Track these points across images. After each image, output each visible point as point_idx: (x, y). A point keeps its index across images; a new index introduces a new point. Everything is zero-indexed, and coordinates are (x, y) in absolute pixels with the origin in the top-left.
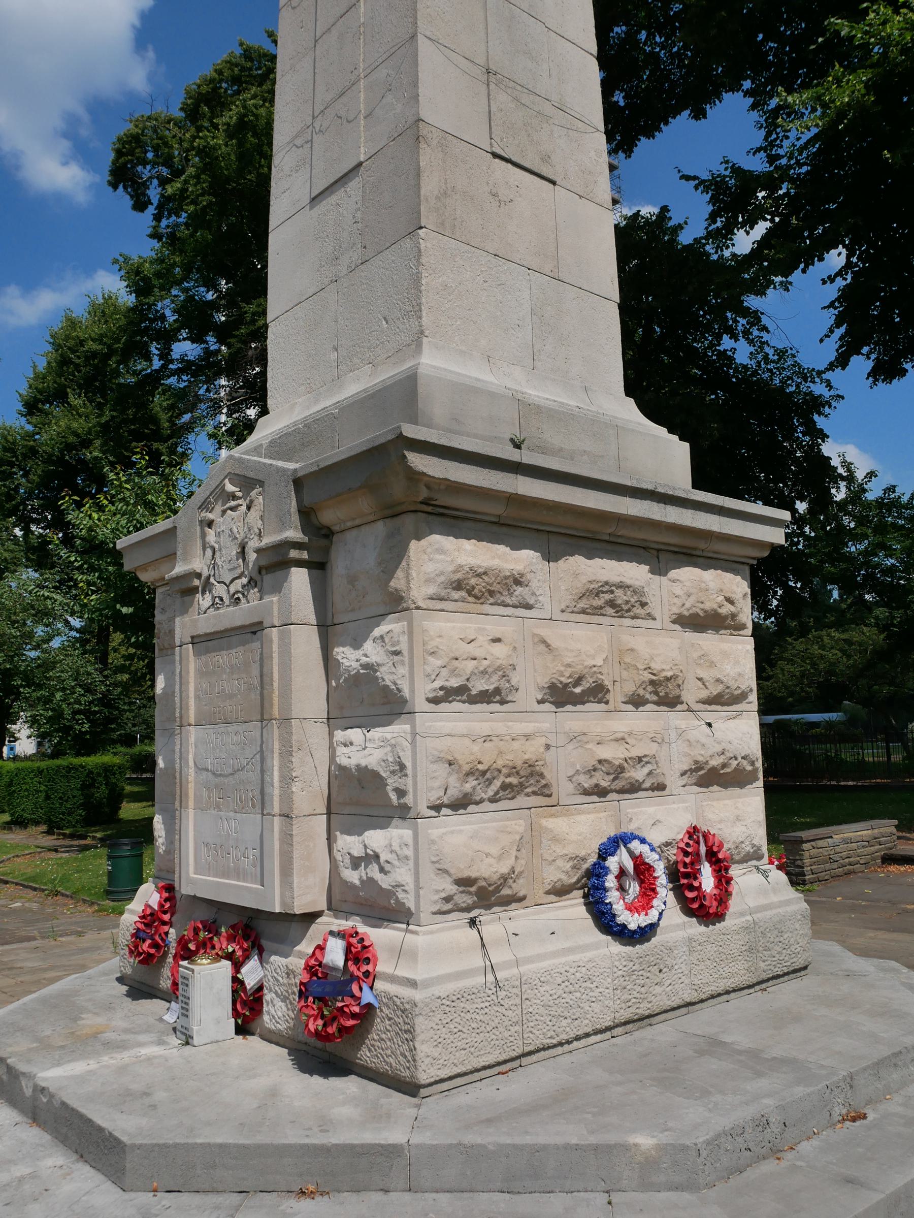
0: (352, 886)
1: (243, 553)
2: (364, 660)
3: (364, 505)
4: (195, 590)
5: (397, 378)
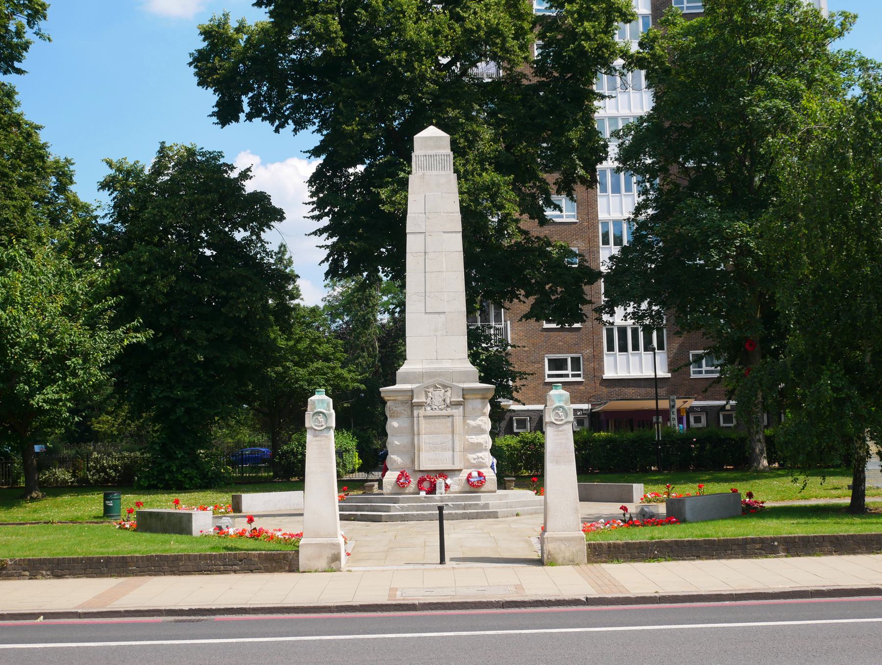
3: (479, 396)
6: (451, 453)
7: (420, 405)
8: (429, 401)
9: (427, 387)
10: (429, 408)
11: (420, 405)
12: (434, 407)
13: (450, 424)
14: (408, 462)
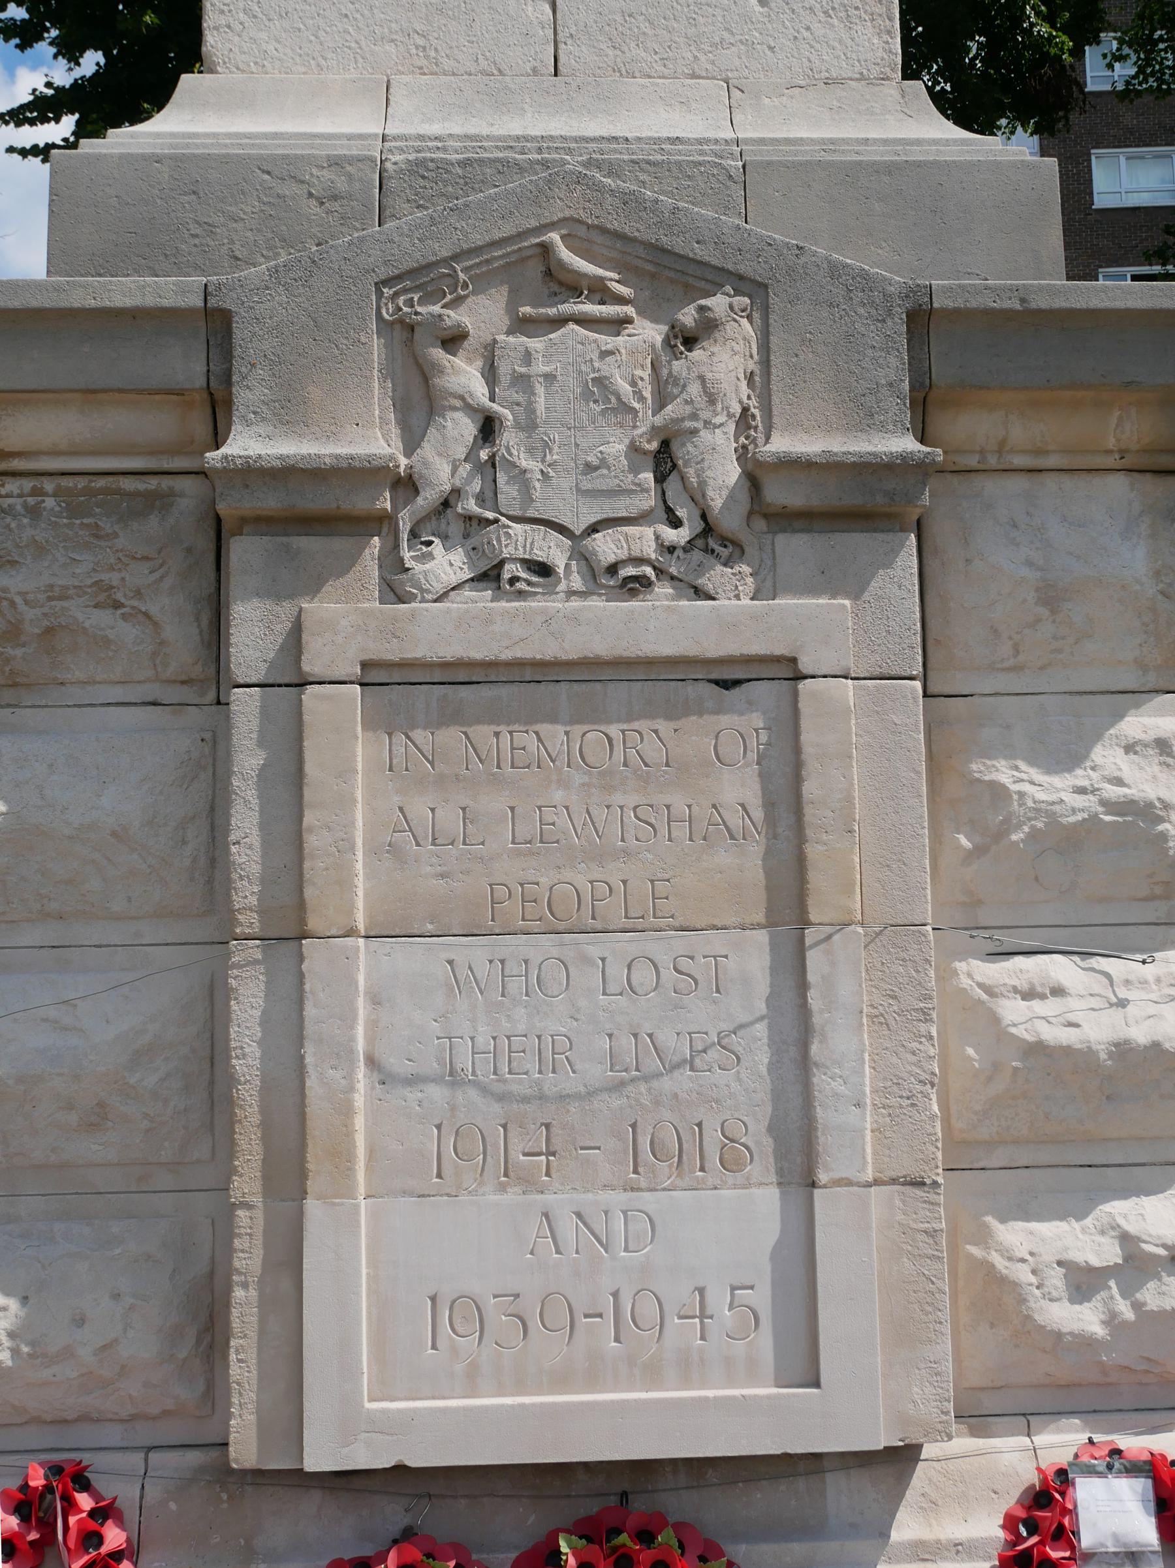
0: (1085, 1342)
1: (664, 459)
2: (1113, 792)
3: (1127, 428)
4: (382, 522)
5: (917, 155)
6: (766, 1202)
7: (325, 515)
8: (444, 458)
9: (429, 278)
10: (446, 564)
11: (325, 515)
12: (518, 541)
13: (740, 790)
14: (123, 1330)
